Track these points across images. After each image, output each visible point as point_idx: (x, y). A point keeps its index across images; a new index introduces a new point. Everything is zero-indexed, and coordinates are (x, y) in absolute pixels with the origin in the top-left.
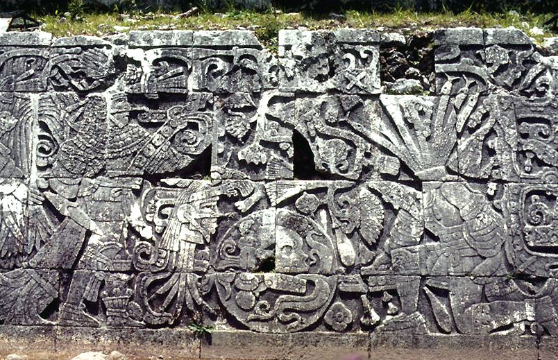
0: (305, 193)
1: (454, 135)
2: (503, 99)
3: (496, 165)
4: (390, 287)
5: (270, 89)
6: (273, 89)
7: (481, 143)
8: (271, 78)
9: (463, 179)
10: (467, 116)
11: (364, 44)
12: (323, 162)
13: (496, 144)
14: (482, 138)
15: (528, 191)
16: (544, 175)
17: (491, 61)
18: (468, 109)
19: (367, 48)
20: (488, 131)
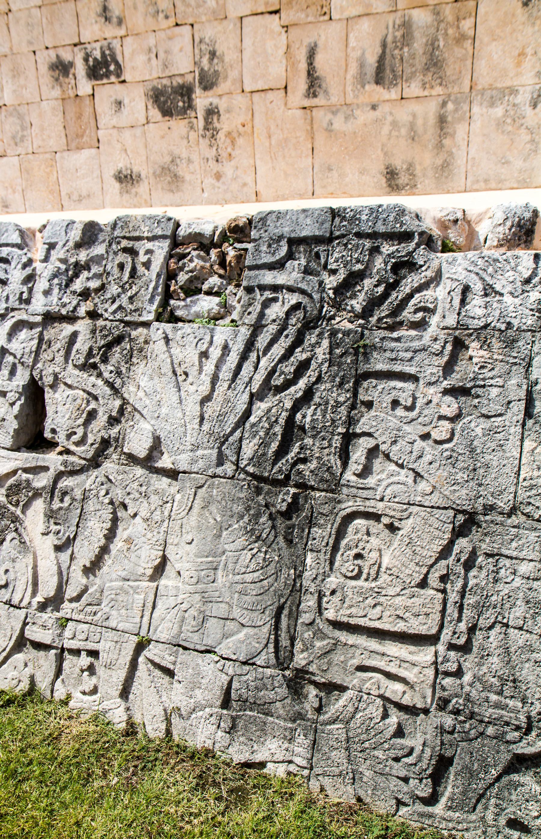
0: (20, 472)
1: (246, 397)
2: (340, 335)
3: (302, 456)
4: (91, 646)
5: (16, 309)
6: (20, 309)
7: (285, 414)
8: (22, 293)
9: (242, 476)
10: (272, 364)
11: (149, 239)
12: (53, 426)
13: (308, 419)
14: (288, 405)
15: (349, 510)
16: (385, 483)
17: (334, 266)
18: (278, 350)
19: (149, 245)
20: (300, 394)
